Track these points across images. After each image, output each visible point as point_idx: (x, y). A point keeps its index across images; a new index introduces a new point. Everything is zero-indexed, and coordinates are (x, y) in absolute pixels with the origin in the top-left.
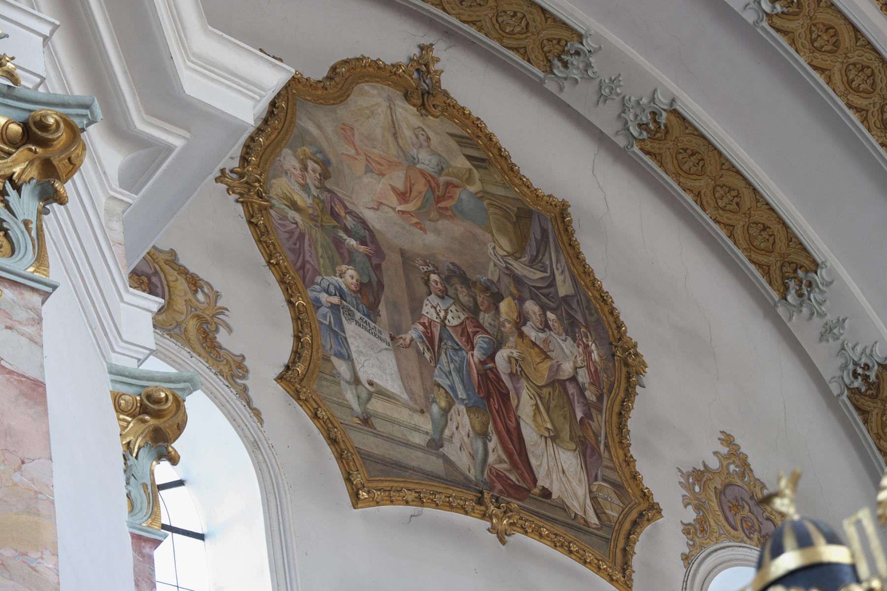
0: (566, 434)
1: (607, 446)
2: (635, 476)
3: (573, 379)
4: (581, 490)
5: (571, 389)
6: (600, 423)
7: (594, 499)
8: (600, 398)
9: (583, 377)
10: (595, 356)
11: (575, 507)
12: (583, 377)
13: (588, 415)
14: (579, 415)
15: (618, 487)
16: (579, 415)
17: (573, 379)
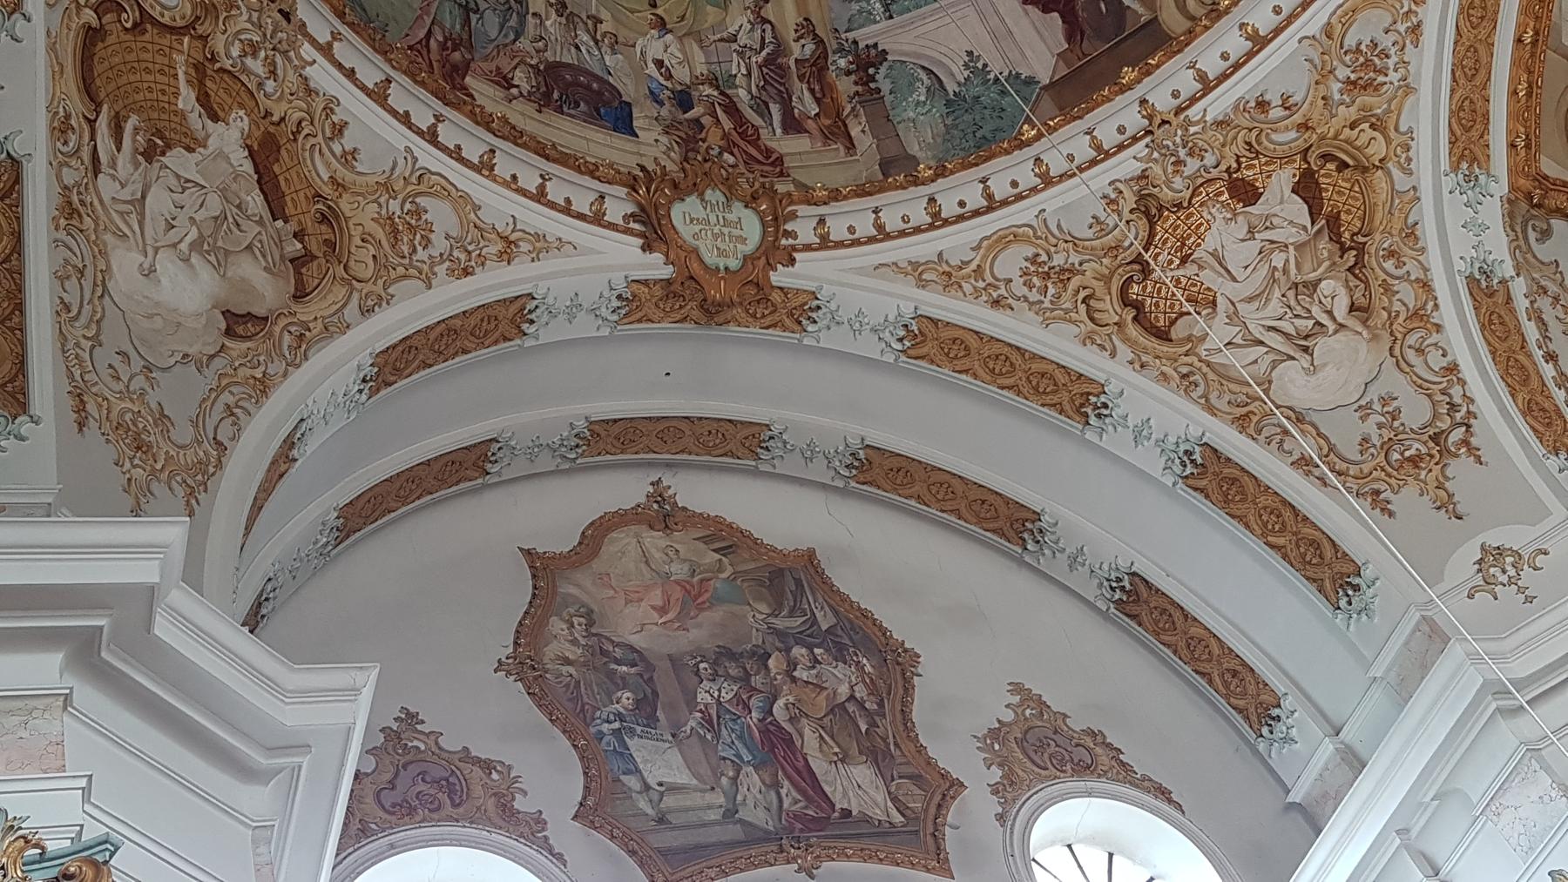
0: (854, 750)
1: (896, 744)
2: (929, 762)
3: (852, 697)
4: (881, 796)
5: (851, 708)
6: (886, 726)
7: (895, 800)
8: (881, 704)
9: (860, 692)
10: (868, 668)
11: (878, 814)
12: (860, 692)
13: (873, 724)
14: (863, 728)
15: (916, 779)
16: (863, 728)
17: (852, 697)
